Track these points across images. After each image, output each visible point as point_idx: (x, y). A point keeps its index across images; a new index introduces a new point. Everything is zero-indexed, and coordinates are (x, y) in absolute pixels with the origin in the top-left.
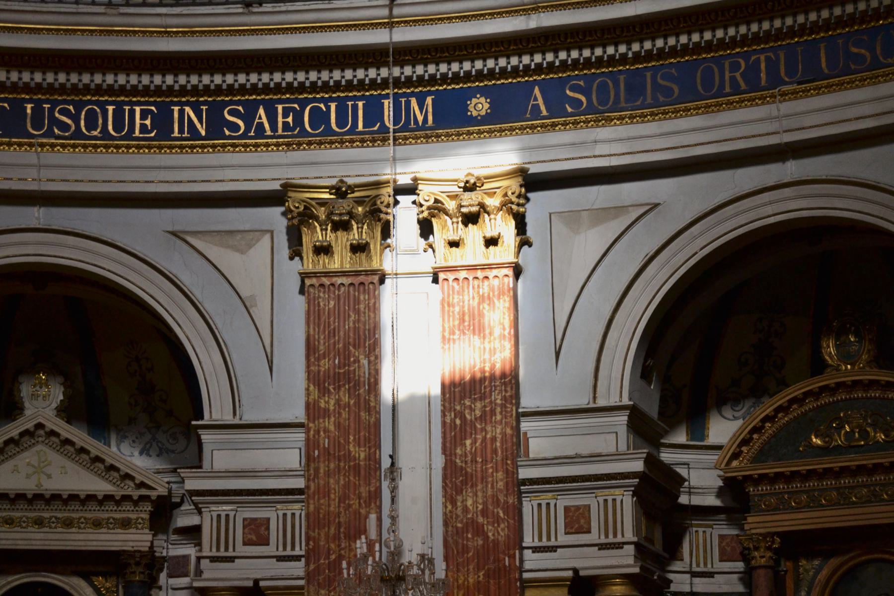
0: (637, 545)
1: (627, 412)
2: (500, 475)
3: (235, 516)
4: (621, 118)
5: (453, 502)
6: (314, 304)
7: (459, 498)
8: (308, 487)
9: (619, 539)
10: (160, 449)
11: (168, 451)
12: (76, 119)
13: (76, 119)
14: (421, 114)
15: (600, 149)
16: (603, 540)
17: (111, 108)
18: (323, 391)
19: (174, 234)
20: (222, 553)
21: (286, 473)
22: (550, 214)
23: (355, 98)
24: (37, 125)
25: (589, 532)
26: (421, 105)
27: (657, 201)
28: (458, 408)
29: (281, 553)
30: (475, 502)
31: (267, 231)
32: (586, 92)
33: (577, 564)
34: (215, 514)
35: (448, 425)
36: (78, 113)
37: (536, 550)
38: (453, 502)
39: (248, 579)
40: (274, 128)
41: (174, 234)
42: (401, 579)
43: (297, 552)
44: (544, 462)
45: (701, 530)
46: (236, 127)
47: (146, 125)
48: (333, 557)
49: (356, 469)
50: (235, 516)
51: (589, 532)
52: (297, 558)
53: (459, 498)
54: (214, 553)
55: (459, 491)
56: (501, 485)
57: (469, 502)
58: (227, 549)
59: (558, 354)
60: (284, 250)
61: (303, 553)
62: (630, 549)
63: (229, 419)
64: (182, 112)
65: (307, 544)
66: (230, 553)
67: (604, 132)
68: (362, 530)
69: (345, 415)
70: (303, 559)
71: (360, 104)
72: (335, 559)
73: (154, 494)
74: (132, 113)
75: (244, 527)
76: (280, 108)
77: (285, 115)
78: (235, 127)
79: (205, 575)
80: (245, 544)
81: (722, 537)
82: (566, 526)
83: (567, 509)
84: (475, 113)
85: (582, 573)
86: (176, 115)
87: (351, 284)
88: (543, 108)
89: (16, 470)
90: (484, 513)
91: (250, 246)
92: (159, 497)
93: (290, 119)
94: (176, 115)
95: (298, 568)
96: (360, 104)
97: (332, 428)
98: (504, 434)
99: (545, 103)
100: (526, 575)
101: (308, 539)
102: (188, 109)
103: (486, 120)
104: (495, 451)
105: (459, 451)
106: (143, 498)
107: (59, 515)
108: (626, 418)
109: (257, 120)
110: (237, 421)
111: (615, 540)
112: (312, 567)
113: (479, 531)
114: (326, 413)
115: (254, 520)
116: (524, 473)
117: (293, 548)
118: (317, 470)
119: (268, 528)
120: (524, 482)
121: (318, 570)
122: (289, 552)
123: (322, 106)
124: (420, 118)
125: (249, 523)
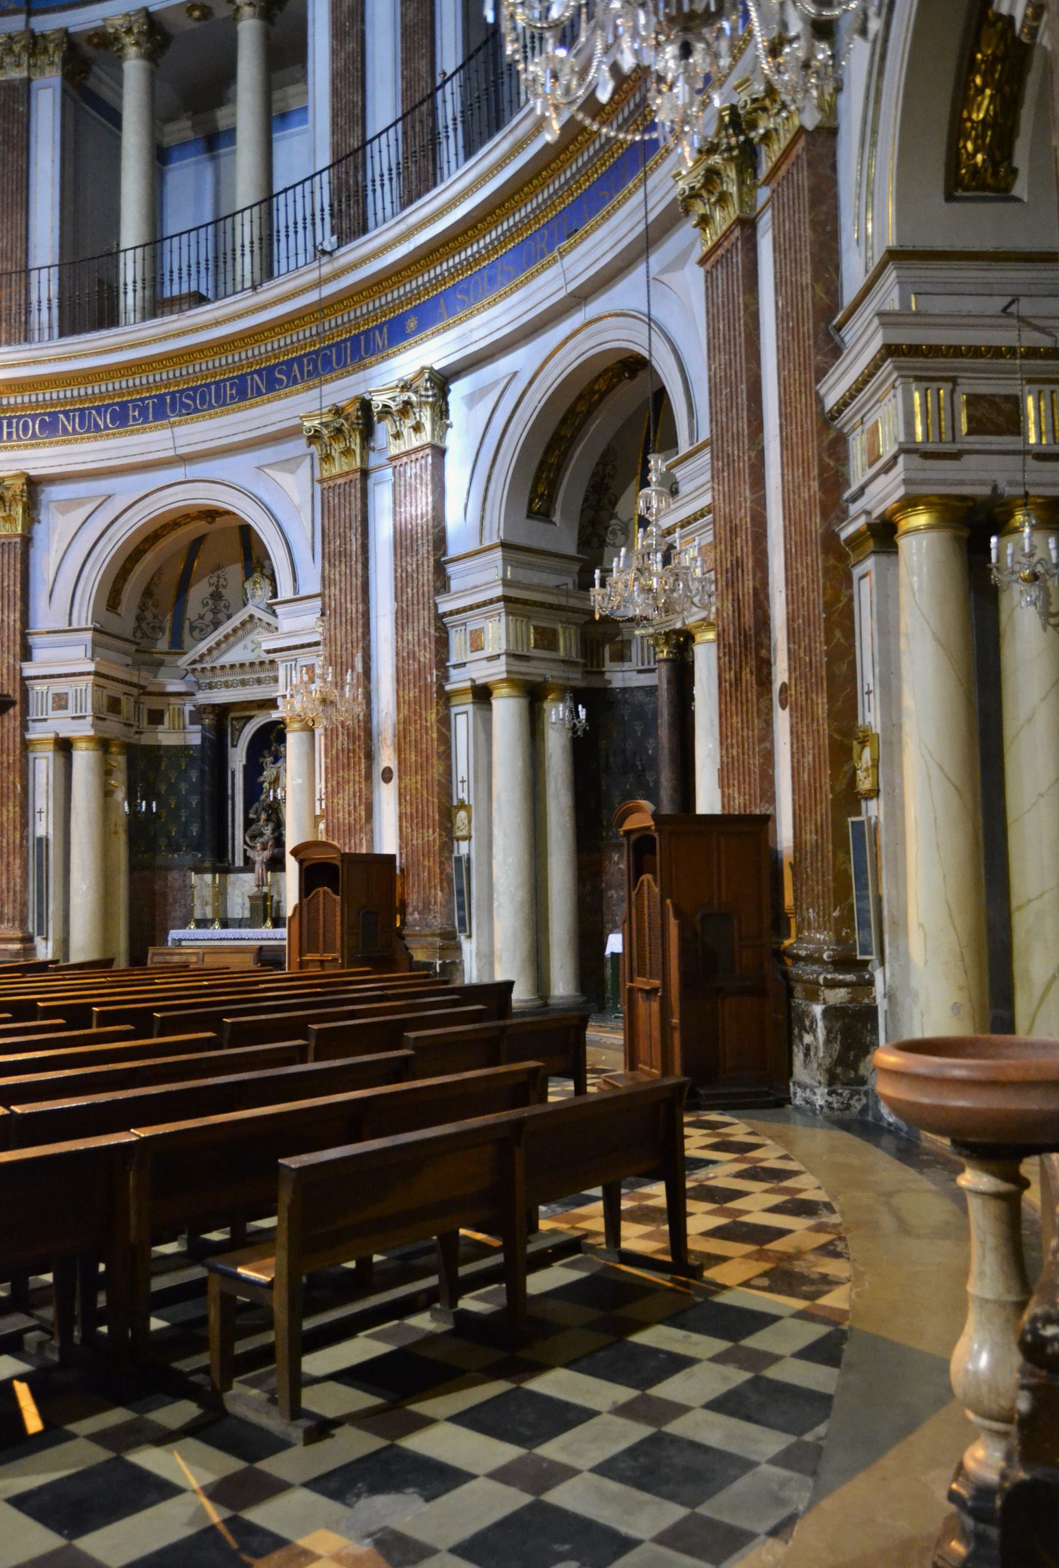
0: (510, 655)
2: (426, 612)
12: (194, 400)
13: (194, 400)
15: (476, 336)
17: (213, 387)
18: (332, 565)
19: (258, 468)
24: (173, 410)
36: (195, 394)
40: (302, 378)
41: (258, 468)
62: (503, 658)
64: (252, 379)
82: (471, 645)
85: (478, 682)
89: (245, 647)
91: (297, 468)
116: (443, 608)
120: (445, 615)
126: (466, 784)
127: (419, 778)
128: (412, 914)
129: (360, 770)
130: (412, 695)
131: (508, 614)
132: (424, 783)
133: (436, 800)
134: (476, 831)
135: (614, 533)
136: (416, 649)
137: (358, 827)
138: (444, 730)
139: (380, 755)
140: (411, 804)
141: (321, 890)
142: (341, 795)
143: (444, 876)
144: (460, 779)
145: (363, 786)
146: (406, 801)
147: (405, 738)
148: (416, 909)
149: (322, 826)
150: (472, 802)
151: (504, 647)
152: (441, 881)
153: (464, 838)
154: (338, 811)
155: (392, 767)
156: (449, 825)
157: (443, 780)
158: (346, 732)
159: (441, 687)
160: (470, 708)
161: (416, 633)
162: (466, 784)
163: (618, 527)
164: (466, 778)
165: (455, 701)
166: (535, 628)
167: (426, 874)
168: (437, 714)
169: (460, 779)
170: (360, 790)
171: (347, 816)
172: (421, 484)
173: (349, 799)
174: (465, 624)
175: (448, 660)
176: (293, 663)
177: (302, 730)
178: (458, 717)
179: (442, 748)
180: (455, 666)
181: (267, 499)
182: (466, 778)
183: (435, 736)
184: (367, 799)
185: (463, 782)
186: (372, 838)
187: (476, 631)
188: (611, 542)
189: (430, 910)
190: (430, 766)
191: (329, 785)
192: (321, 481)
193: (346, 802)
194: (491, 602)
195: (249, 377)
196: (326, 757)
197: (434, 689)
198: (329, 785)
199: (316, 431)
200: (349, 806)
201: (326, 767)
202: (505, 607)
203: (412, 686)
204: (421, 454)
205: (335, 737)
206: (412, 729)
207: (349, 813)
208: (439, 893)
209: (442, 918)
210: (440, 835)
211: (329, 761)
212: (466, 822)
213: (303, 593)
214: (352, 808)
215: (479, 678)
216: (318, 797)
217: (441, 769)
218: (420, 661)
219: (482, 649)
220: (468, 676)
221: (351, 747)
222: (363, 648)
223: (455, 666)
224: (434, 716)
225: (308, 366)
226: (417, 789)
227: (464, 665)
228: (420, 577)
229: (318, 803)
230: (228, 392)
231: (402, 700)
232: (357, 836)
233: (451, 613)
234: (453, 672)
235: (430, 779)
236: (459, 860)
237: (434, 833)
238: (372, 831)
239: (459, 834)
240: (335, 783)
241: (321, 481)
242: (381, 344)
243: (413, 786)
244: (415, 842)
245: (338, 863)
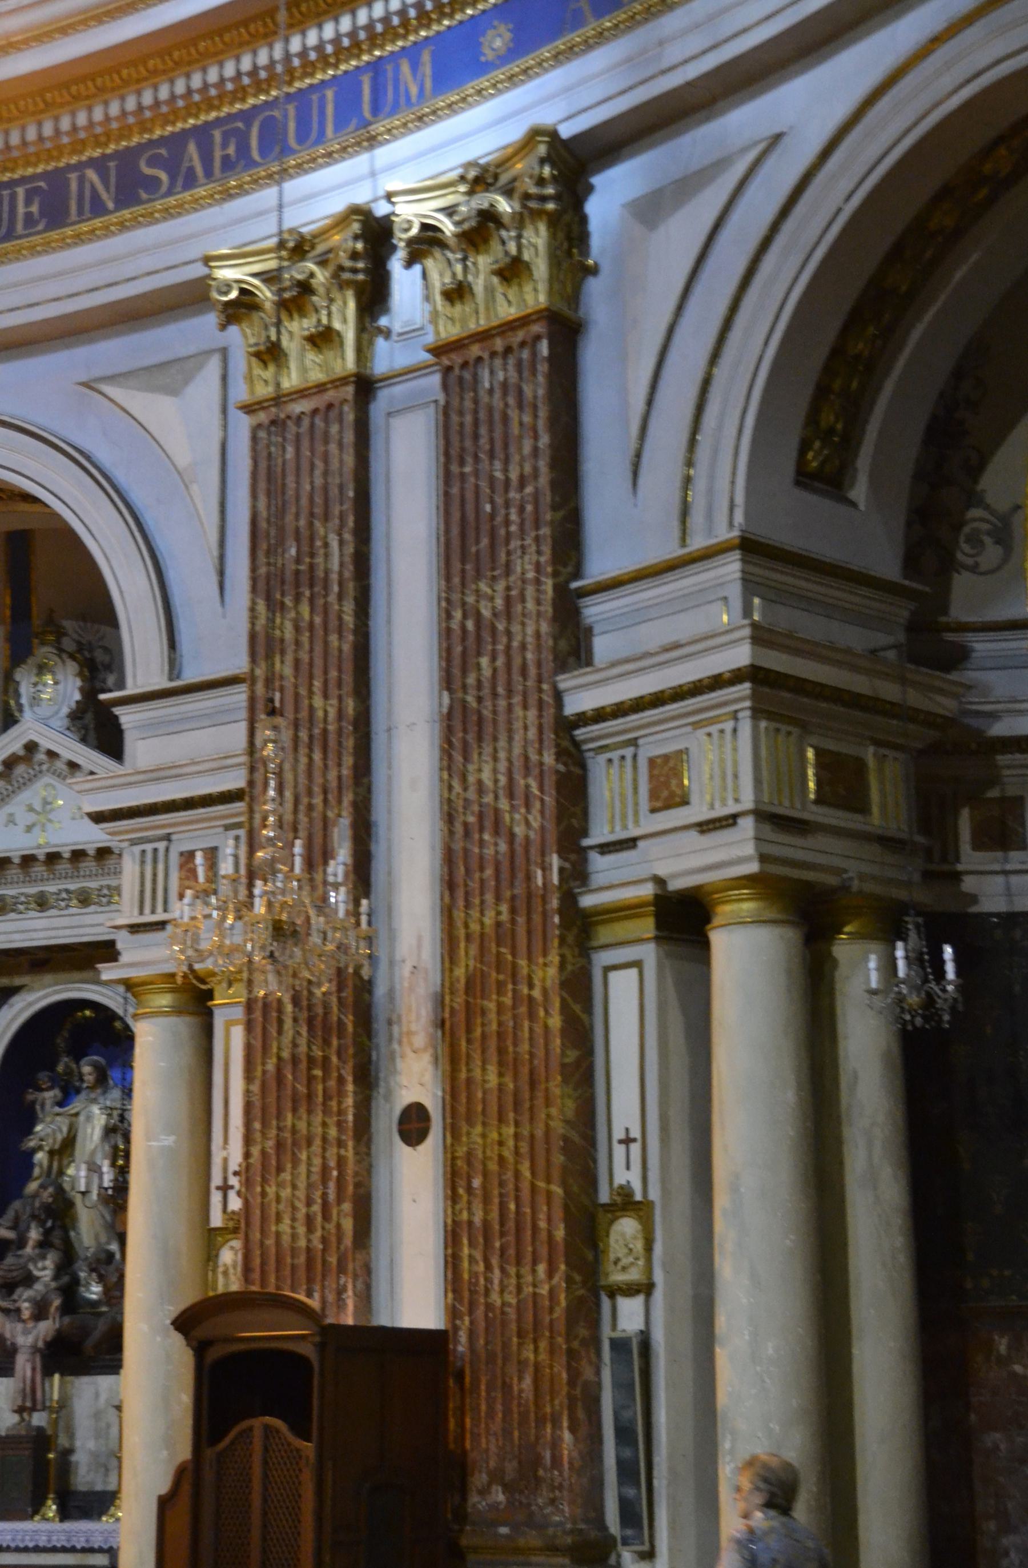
0: (762, 816)
2: (532, 714)
3: (167, 850)
9: (732, 808)
15: (674, 53)
19: (86, 385)
28: (471, 599)
40: (209, 173)
41: (86, 385)
50: (167, 850)
62: (747, 825)
64: (82, 180)
74: (13, 197)
79: (124, 958)
82: (653, 795)
85: (674, 885)
86: (74, 186)
87: (315, 411)
91: (187, 382)
94: (74, 186)
107: (72, 887)
116: (577, 703)
120: (583, 719)
126: (635, 1148)
127: (511, 1130)
128: (484, 1492)
129: (340, 1112)
130: (488, 921)
131: (757, 713)
132: (524, 1147)
133: (557, 1190)
134: (667, 1272)
135: (975, 540)
136: (504, 804)
137: (333, 1260)
138: (577, 1008)
139: (394, 1072)
140: (486, 1201)
141: (258, 1423)
142: (286, 1176)
143: (578, 1391)
144: (618, 1134)
145: (349, 1153)
146: (469, 1189)
147: (469, 1030)
148: (497, 1477)
149: (229, 1256)
150: (654, 1194)
151: (748, 801)
152: (572, 1400)
153: (631, 1290)
154: (279, 1219)
156: (590, 1256)
157: (576, 1138)
158: (304, 1015)
159: (569, 899)
160: (648, 953)
161: (502, 766)
162: (635, 1148)
163: (985, 526)
164: (636, 1133)
165: (604, 934)
166: (819, 753)
167: (528, 1382)
168: (562, 966)
169: (618, 1134)
170: (341, 1162)
171: (301, 1230)
172: (520, 407)
173: (310, 1186)
174: (634, 742)
175: (585, 833)
176: (161, 846)
177: (177, 1011)
178: (613, 976)
179: (572, 1055)
180: (606, 848)
181: (104, 455)
182: (636, 1133)
183: (555, 1022)
184: (357, 1185)
185: (627, 1141)
186: (368, 1287)
187: (666, 757)
188: (970, 561)
189: (538, 1480)
190: (540, 1101)
191: (256, 1151)
192: (249, 409)
193: (301, 1194)
194: (717, 682)
195: (73, 176)
196: (249, 1075)
197: (555, 903)
198: (256, 1151)
199: (243, 292)
200: (309, 1203)
201: (248, 1107)
202: (754, 696)
203: (489, 897)
204: (520, 335)
205: (273, 1031)
206: (491, 1006)
207: (309, 1220)
208: (567, 1436)
209: (572, 1503)
210: (569, 1280)
211: (255, 1088)
212: (639, 1246)
213: (191, 675)
214: (316, 1208)
215: (675, 876)
216: (217, 1180)
217: (570, 1105)
218: (512, 836)
219: (685, 802)
220: (645, 871)
221: (318, 1053)
222: (355, 804)
223: (606, 848)
224: (552, 971)
225: (225, 145)
226: (501, 1159)
227: (630, 843)
228: (516, 628)
229: (216, 1198)
230: (21, 209)
231: (461, 933)
232: (331, 1283)
233: (600, 715)
234: (598, 862)
235: (539, 1133)
236: (620, 1346)
237: (551, 1273)
238: (368, 1270)
239: (618, 1277)
240: (270, 1144)
241: (249, 409)
242: (414, 90)
243: (493, 1153)
244: (495, 1298)
245: (307, 1350)
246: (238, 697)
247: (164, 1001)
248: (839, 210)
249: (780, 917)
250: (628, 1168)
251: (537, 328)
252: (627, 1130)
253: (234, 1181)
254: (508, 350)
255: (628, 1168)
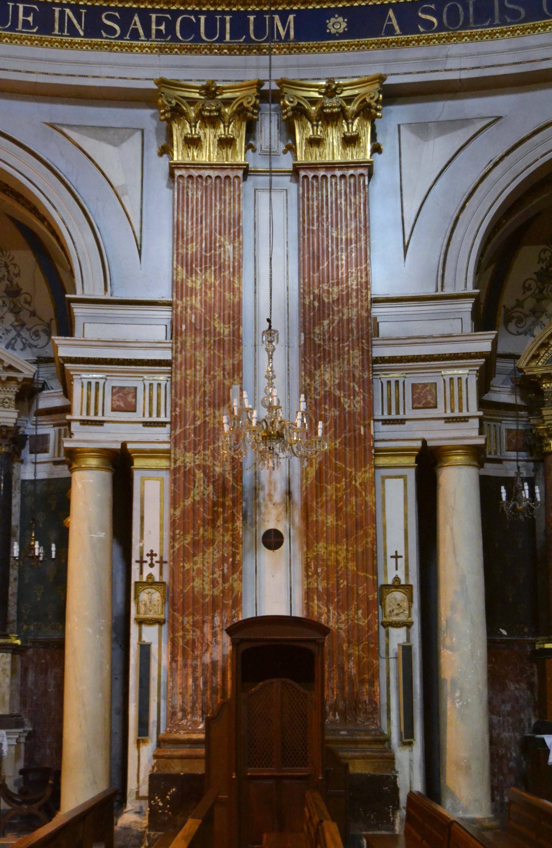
1: (473, 300)
2: (356, 353)
3: (104, 384)
4: (472, 37)
5: (311, 376)
6: (183, 193)
7: (318, 373)
8: (175, 358)
9: (465, 413)
10: (24, 344)
11: (31, 346)
14: (284, 28)
15: (452, 64)
16: (449, 414)
18: (191, 272)
20: (92, 417)
21: (154, 345)
22: (399, 126)
23: (223, 12)
25: (435, 407)
26: (284, 22)
27: (499, 115)
28: (316, 291)
29: (147, 419)
30: (333, 377)
31: (137, 129)
32: (437, 14)
33: (426, 436)
34: (85, 382)
35: (307, 306)
37: (386, 422)
38: (311, 376)
39: (116, 441)
42: (280, 436)
43: (162, 419)
44: (397, 342)
45: (492, 424)
46: (114, 31)
47: (28, 22)
48: (198, 423)
49: (220, 343)
50: (104, 384)
51: (435, 407)
52: (162, 424)
53: (318, 373)
54: (84, 417)
55: (317, 366)
56: (357, 361)
57: (327, 376)
58: (96, 414)
59: (406, 248)
60: (153, 148)
61: (168, 419)
63: (100, 294)
64: (62, 13)
65: (173, 410)
66: (99, 418)
67: (454, 49)
68: (225, 400)
69: (210, 294)
70: (168, 426)
71: (228, 18)
72: (200, 426)
73: (20, 377)
74: (16, 9)
75: (113, 394)
76: (154, 16)
77: (158, 23)
78: (111, 31)
79: (76, 437)
80: (113, 410)
81: (509, 431)
83: (414, 386)
84: (333, 31)
85: (430, 444)
86: (57, 15)
87: (218, 177)
88: (397, 28)
90: (340, 386)
91: (123, 141)
92: (25, 379)
93: (163, 27)
94: (57, 15)
95: (163, 434)
96: (228, 18)
97: (198, 306)
98: (359, 316)
99: (399, 24)
100: (379, 445)
101: (174, 405)
102: (68, 11)
103: (343, 36)
104: (351, 331)
105: (317, 331)
106: (9, 379)
108: (470, 306)
109: (132, 26)
110: (108, 297)
111: (461, 415)
112: (178, 431)
113: (336, 403)
114: (192, 291)
115: (122, 388)
116: (377, 352)
117: (158, 415)
118: (183, 344)
119: (135, 397)
120: (378, 360)
121: (185, 435)
122: (154, 419)
123: (192, 18)
124: (283, 33)
125: (117, 391)
144: (391, 552)
148: (335, 708)
155: (281, 529)
164: (401, 553)
169: (391, 552)
171: (207, 587)
182: (401, 553)
204: (351, 172)
211: (178, 513)
212: (405, 604)
216: (135, 556)
229: (135, 567)
246: (165, 314)
247: (93, 462)
248: (537, 160)
249: (476, 464)
250: (397, 569)
251: (360, 171)
252: (396, 552)
253: (146, 558)
254: (343, 176)
255: (397, 569)
